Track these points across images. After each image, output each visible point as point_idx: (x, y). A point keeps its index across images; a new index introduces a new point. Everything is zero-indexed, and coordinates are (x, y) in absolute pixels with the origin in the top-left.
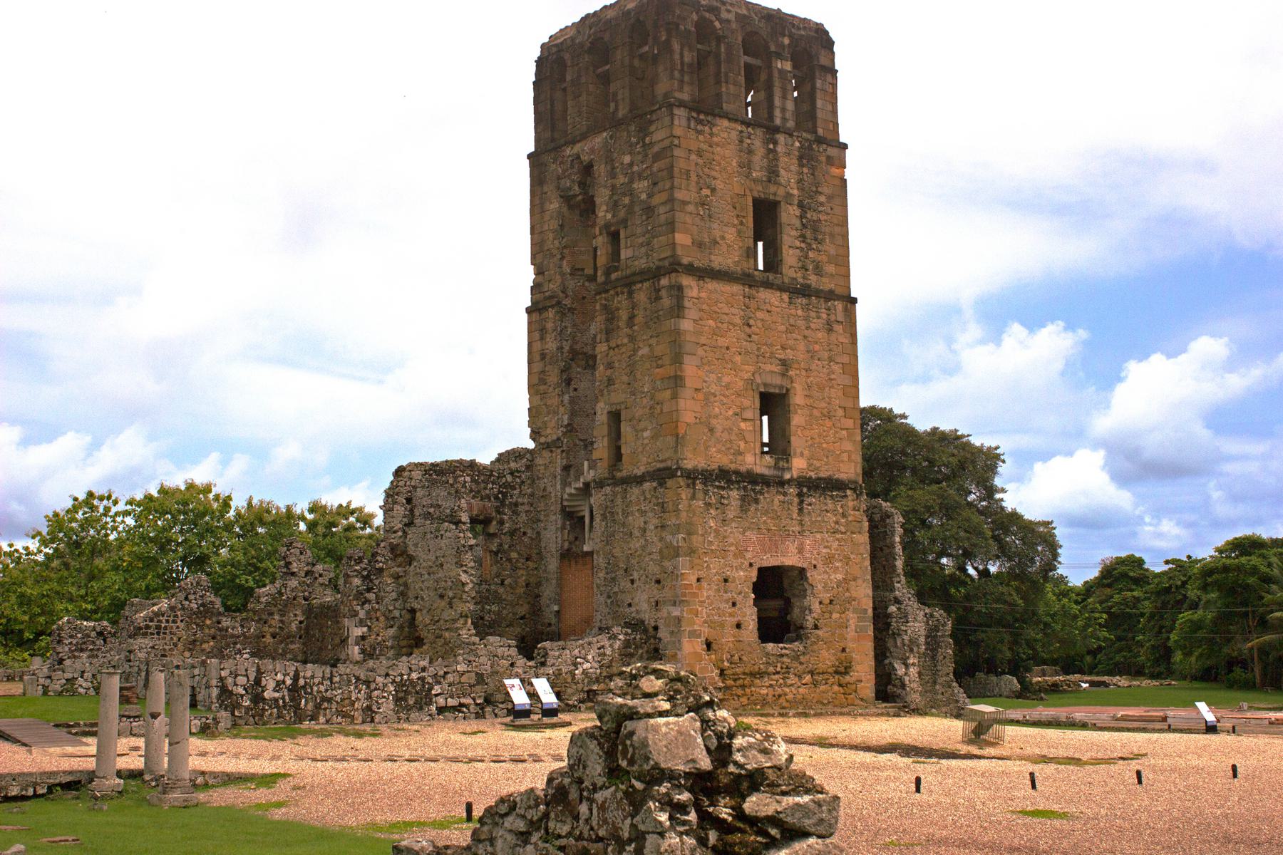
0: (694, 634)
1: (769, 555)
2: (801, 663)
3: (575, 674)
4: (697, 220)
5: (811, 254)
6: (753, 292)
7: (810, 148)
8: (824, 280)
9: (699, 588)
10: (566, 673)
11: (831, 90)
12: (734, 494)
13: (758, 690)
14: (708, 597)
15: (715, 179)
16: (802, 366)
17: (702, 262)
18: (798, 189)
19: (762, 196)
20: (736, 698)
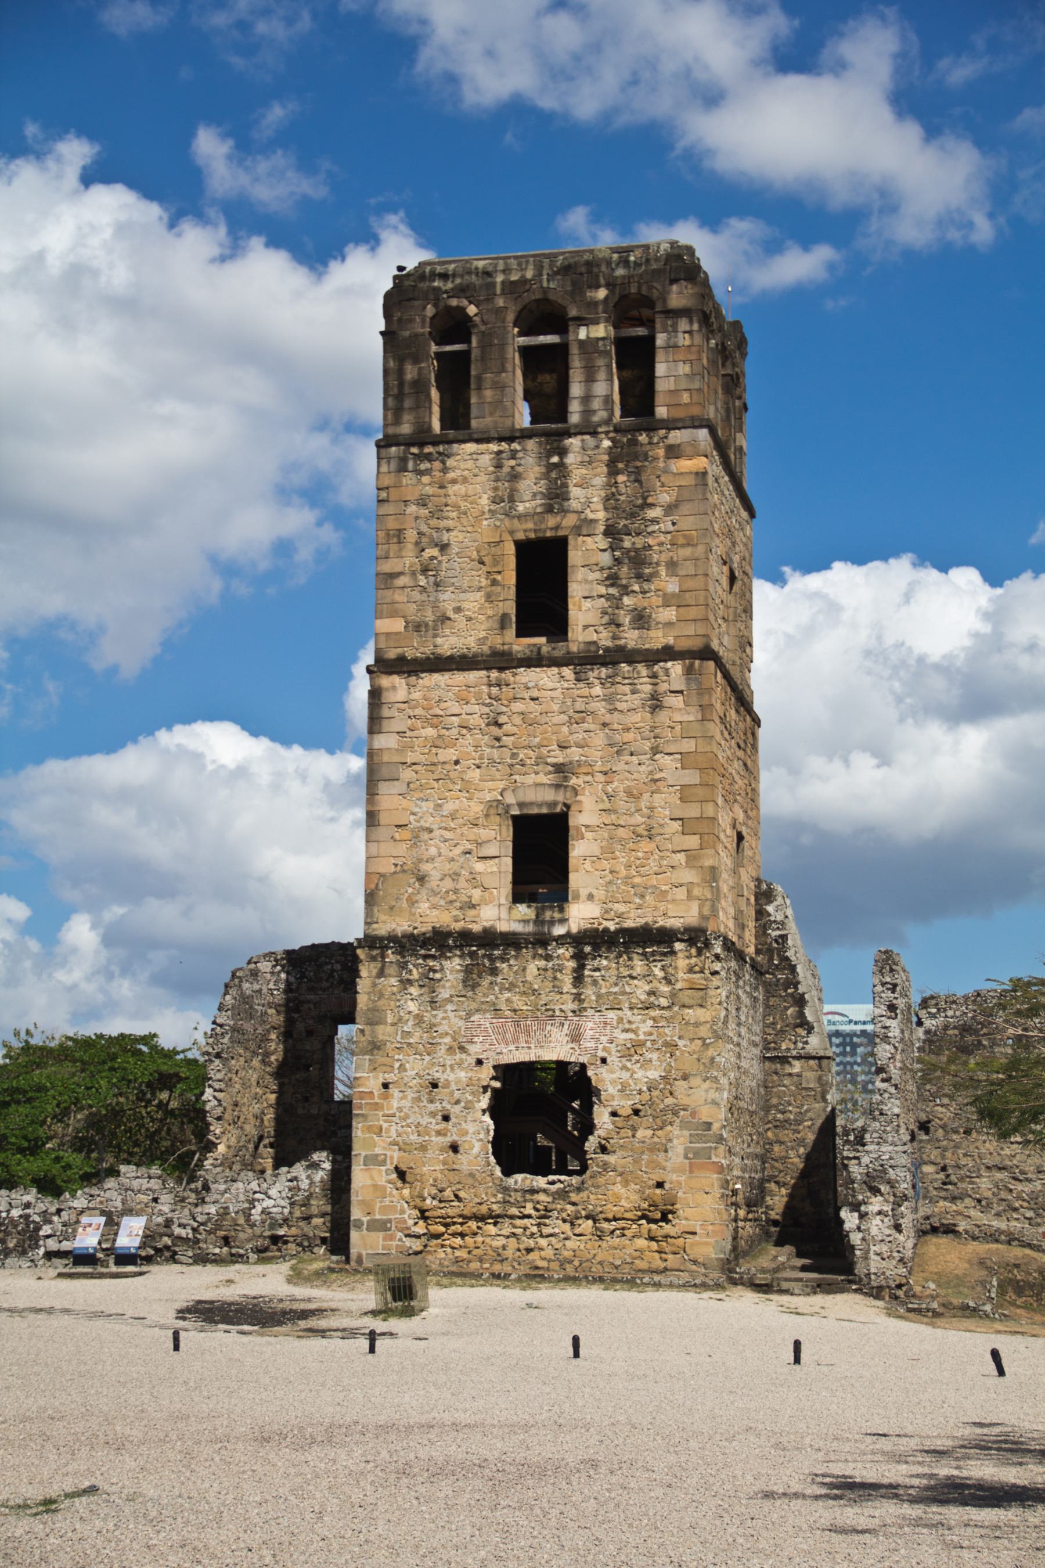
0: (373, 1160)
1: (512, 1047)
2: (574, 1204)
3: (250, 1215)
4: (416, 595)
5: (627, 600)
6: (507, 675)
7: (634, 442)
8: (652, 633)
9: (386, 1097)
10: (237, 1213)
11: (687, 343)
12: (453, 967)
13: (488, 1240)
14: (400, 1109)
15: (448, 530)
16: (596, 768)
17: (422, 650)
18: (606, 509)
19: (532, 536)
20: (449, 1250)
